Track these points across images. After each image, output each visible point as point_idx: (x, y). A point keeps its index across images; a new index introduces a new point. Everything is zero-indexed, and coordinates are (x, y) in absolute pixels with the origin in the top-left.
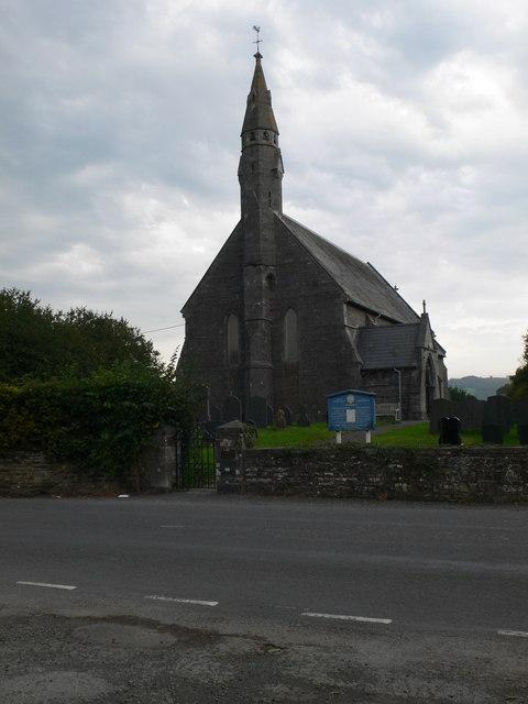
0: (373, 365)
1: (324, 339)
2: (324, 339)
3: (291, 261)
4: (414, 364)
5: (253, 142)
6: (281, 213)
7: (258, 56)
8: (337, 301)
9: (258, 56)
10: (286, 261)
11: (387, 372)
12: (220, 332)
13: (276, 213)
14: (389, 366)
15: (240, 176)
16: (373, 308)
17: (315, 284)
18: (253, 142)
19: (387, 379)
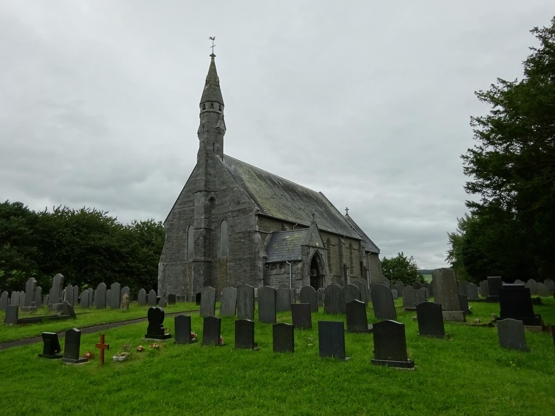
0: (274, 259)
1: (243, 240)
2: (243, 240)
3: (225, 188)
4: (300, 258)
5: (205, 111)
6: (222, 156)
7: (213, 56)
8: (251, 214)
9: (213, 56)
10: (222, 188)
11: (282, 264)
12: (184, 237)
13: (218, 156)
14: (283, 259)
15: (198, 133)
16: (291, 219)
17: (239, 203)
18: (205, 111)
19: (283, 270)
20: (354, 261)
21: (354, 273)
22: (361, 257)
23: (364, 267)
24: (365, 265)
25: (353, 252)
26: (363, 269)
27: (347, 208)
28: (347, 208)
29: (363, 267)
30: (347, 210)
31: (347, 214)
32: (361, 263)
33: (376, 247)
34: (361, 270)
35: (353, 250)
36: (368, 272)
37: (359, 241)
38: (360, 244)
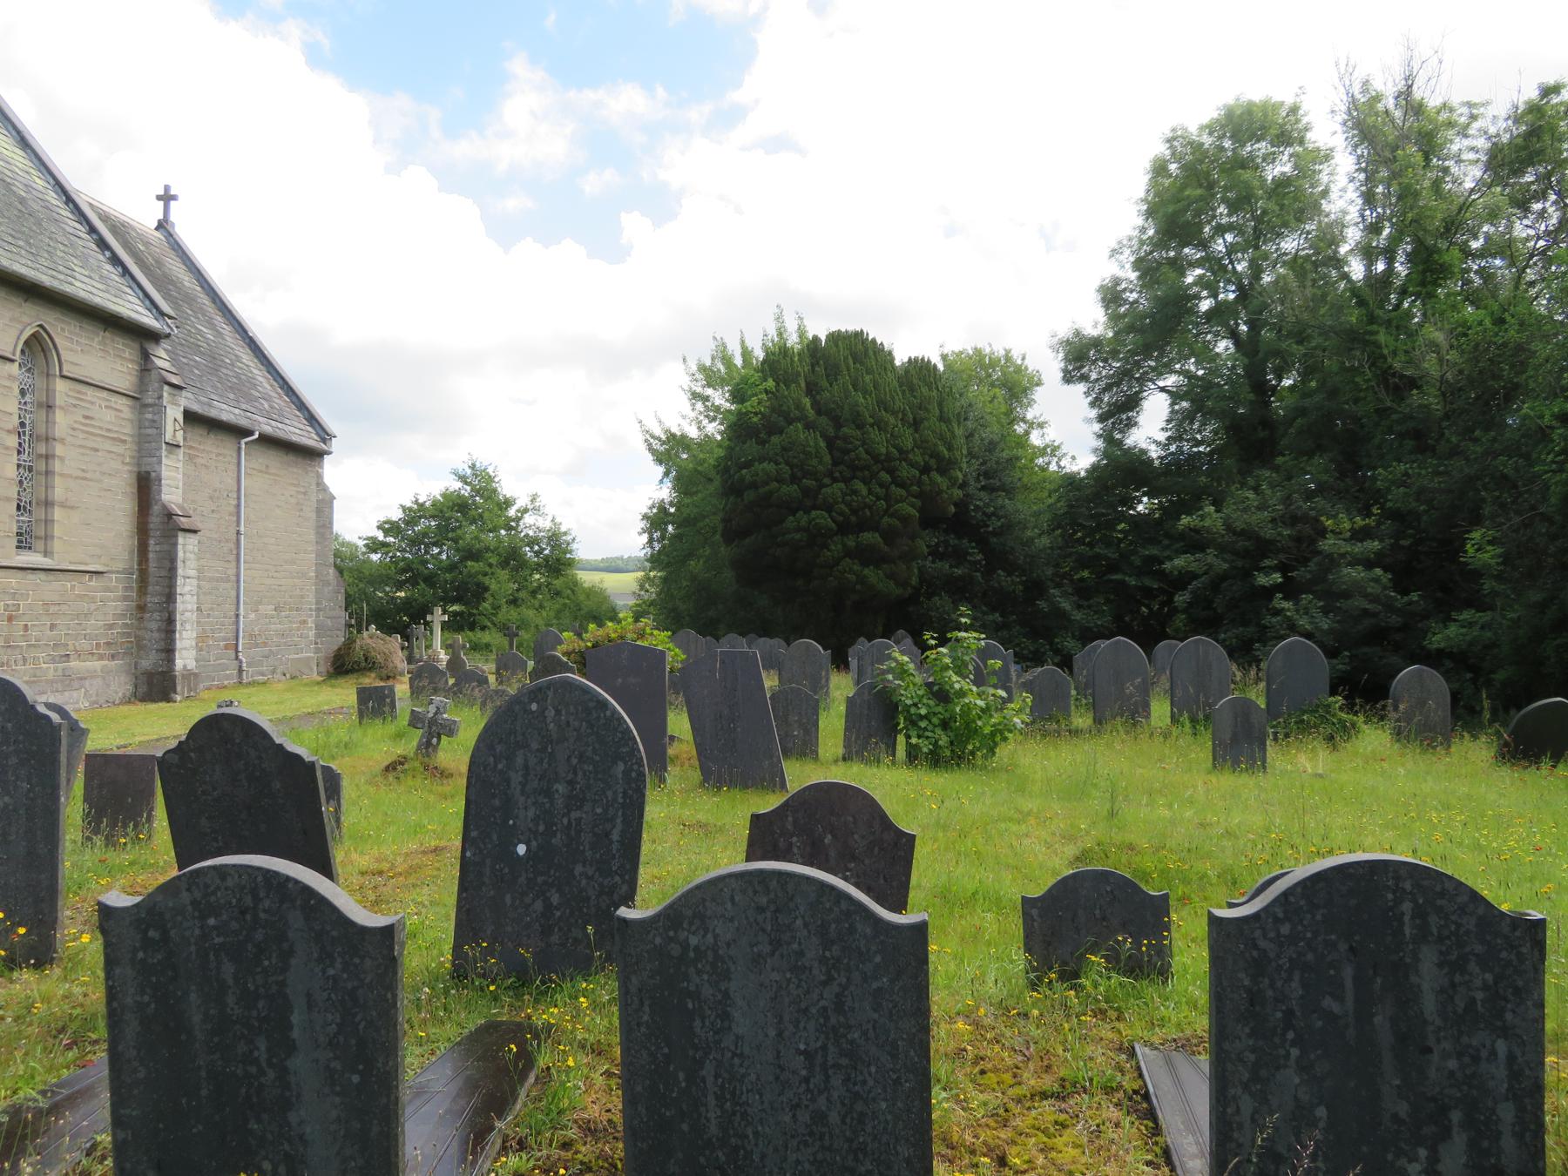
20: (68, 459)
21: (57, 545)
22: (147, 441)
23: (164, 507)
24: (172, 493)
25: (59, 400)
26: (155, 520)
27: (167, 188)
28: (167, 188)
29: (156, 509)
30: (167, 198)
31: (162, 225)
32: (145, 486)
33: (312, 419)
34: (142, 531)
35: (60, 386)
36: (186, 547)
37: (142, 336)
38: (146, 356)
